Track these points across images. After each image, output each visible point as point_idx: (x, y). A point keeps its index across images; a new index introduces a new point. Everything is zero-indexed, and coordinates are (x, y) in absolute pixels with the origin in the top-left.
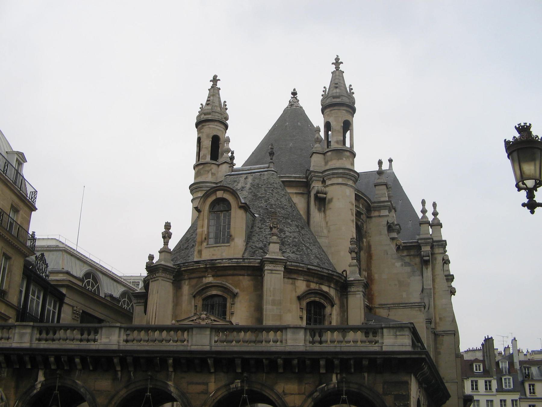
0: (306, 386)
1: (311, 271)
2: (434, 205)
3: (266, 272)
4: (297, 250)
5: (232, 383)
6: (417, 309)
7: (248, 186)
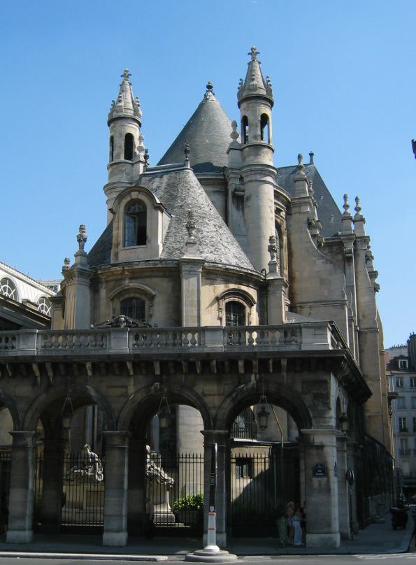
0: (226, 387)
2: (357, 199)
3: (183, 273)
5: (152, 385)
7: (164, 185)
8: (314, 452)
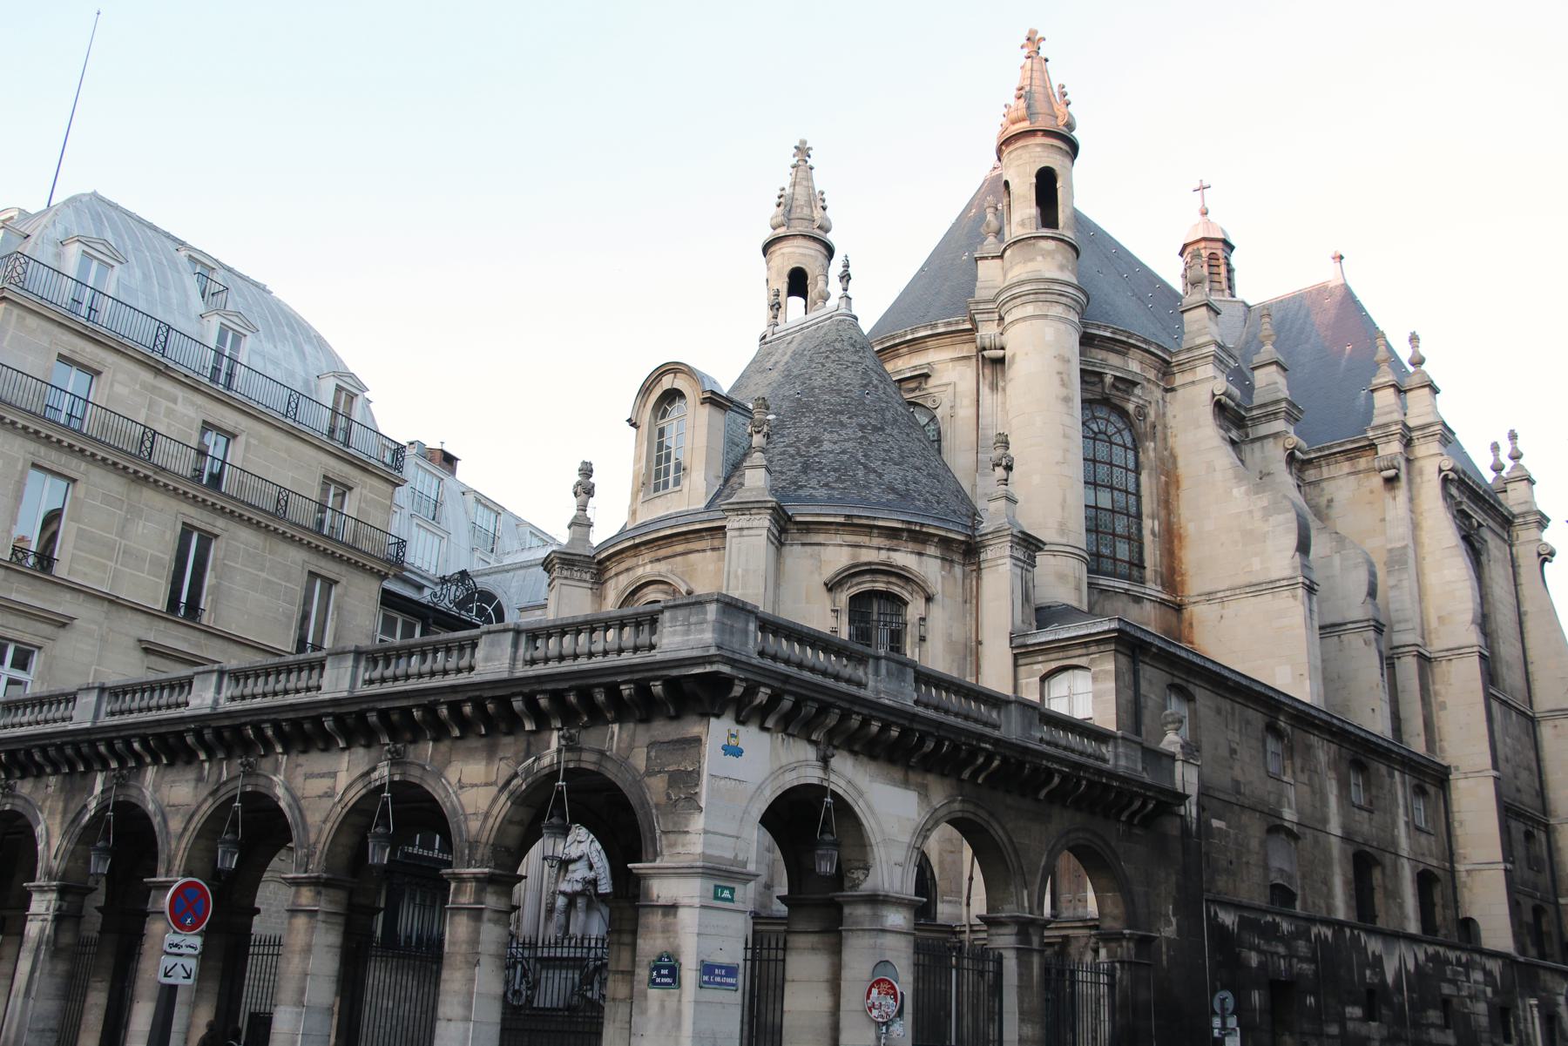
0: (502, 764)
1: (856, 521)
2: (1414, 339)
4: (838, 480)
5: (374, 769)
6: (1287, 593)
7: (786, 358)
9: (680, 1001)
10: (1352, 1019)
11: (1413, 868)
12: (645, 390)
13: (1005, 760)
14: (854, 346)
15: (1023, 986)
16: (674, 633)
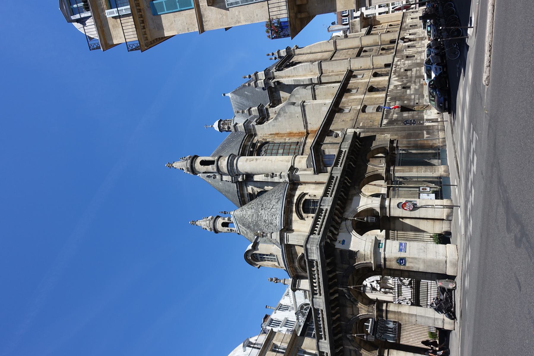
4: (275, 215)
5: (348, 339)
7: (244, 228)
8: (388, 263)
9: (409, 258)
10: (410, 92)
11: (372, 78)
12: (251, 264)
13: (346, 175)
14: (242, 211)
15: (403, 171)
16: (313, 256)
